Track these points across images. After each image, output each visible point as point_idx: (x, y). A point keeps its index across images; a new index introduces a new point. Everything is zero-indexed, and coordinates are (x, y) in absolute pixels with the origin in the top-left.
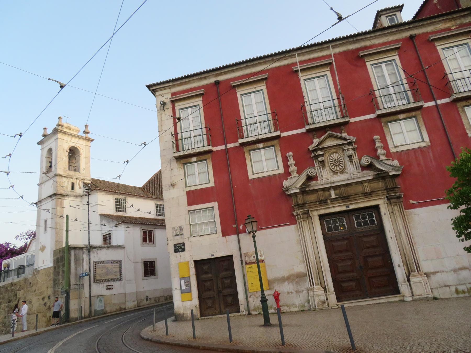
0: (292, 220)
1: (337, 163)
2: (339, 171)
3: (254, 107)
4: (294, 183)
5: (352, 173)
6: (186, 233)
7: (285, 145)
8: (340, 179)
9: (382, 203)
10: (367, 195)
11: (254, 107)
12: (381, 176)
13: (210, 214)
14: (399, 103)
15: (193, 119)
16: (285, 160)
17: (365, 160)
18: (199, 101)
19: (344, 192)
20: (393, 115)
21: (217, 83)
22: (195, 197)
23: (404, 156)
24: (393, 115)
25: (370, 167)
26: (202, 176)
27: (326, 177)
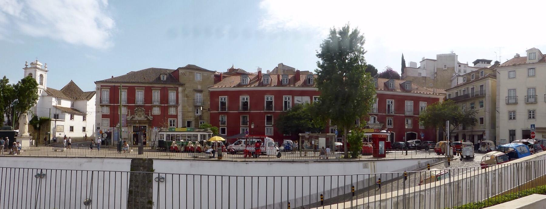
0: (127, 126)
1: (140, 115)
2: (140, 117)
3: (123, 95)
4: (129, 118)
5: (143, 118)
6: (101, 124)
7: (129, 107)
8: (139, 119)
9: (147, 126)
10: (145, 123)
11: (123, 95)
12: (148, 119)
13: (107, 122)
14: (157, 104)
15: (106, 95)
16: (128, 111)
17: (146, 116)
18: (109, 90)
19: (140, 122)
20: (155, 106)
21: (114, 86)
22: (104, 116)
23: (154, 116)
24: (155, 106)
25: (147, 117)
26: (107, 111)
27: (137, 118)
